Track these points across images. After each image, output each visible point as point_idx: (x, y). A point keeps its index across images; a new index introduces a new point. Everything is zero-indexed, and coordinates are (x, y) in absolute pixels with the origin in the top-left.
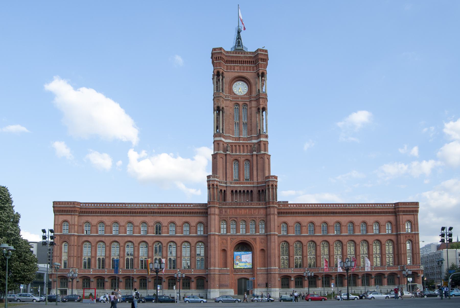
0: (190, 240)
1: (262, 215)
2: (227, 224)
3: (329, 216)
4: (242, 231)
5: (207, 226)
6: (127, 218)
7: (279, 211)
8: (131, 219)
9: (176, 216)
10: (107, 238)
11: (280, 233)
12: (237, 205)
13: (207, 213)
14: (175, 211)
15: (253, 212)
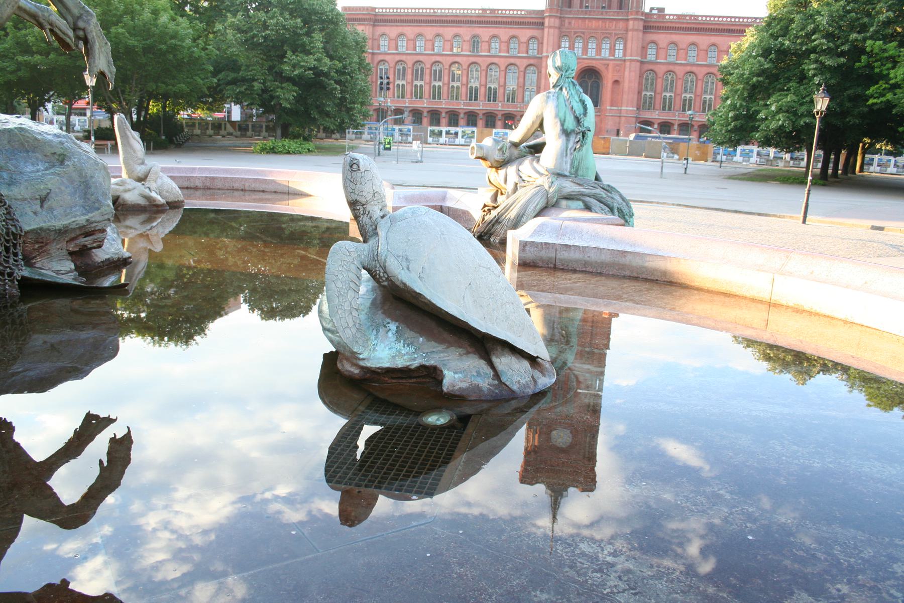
0: (517, 61)
1: (620, 30)
2: (570, 42)
3: (722, 36)
4: (592, 53)
5: (542, 43)
6: (435, 29)
7: (647, 24)
8: (441, 30)
9: (501, 28)
10: (409, 57)
11: (646, 58)
12: (586, 14)
13: (543, 24)
14: (500, 19)
15: (607, 25)
